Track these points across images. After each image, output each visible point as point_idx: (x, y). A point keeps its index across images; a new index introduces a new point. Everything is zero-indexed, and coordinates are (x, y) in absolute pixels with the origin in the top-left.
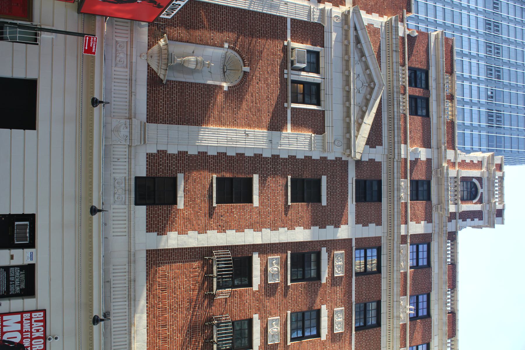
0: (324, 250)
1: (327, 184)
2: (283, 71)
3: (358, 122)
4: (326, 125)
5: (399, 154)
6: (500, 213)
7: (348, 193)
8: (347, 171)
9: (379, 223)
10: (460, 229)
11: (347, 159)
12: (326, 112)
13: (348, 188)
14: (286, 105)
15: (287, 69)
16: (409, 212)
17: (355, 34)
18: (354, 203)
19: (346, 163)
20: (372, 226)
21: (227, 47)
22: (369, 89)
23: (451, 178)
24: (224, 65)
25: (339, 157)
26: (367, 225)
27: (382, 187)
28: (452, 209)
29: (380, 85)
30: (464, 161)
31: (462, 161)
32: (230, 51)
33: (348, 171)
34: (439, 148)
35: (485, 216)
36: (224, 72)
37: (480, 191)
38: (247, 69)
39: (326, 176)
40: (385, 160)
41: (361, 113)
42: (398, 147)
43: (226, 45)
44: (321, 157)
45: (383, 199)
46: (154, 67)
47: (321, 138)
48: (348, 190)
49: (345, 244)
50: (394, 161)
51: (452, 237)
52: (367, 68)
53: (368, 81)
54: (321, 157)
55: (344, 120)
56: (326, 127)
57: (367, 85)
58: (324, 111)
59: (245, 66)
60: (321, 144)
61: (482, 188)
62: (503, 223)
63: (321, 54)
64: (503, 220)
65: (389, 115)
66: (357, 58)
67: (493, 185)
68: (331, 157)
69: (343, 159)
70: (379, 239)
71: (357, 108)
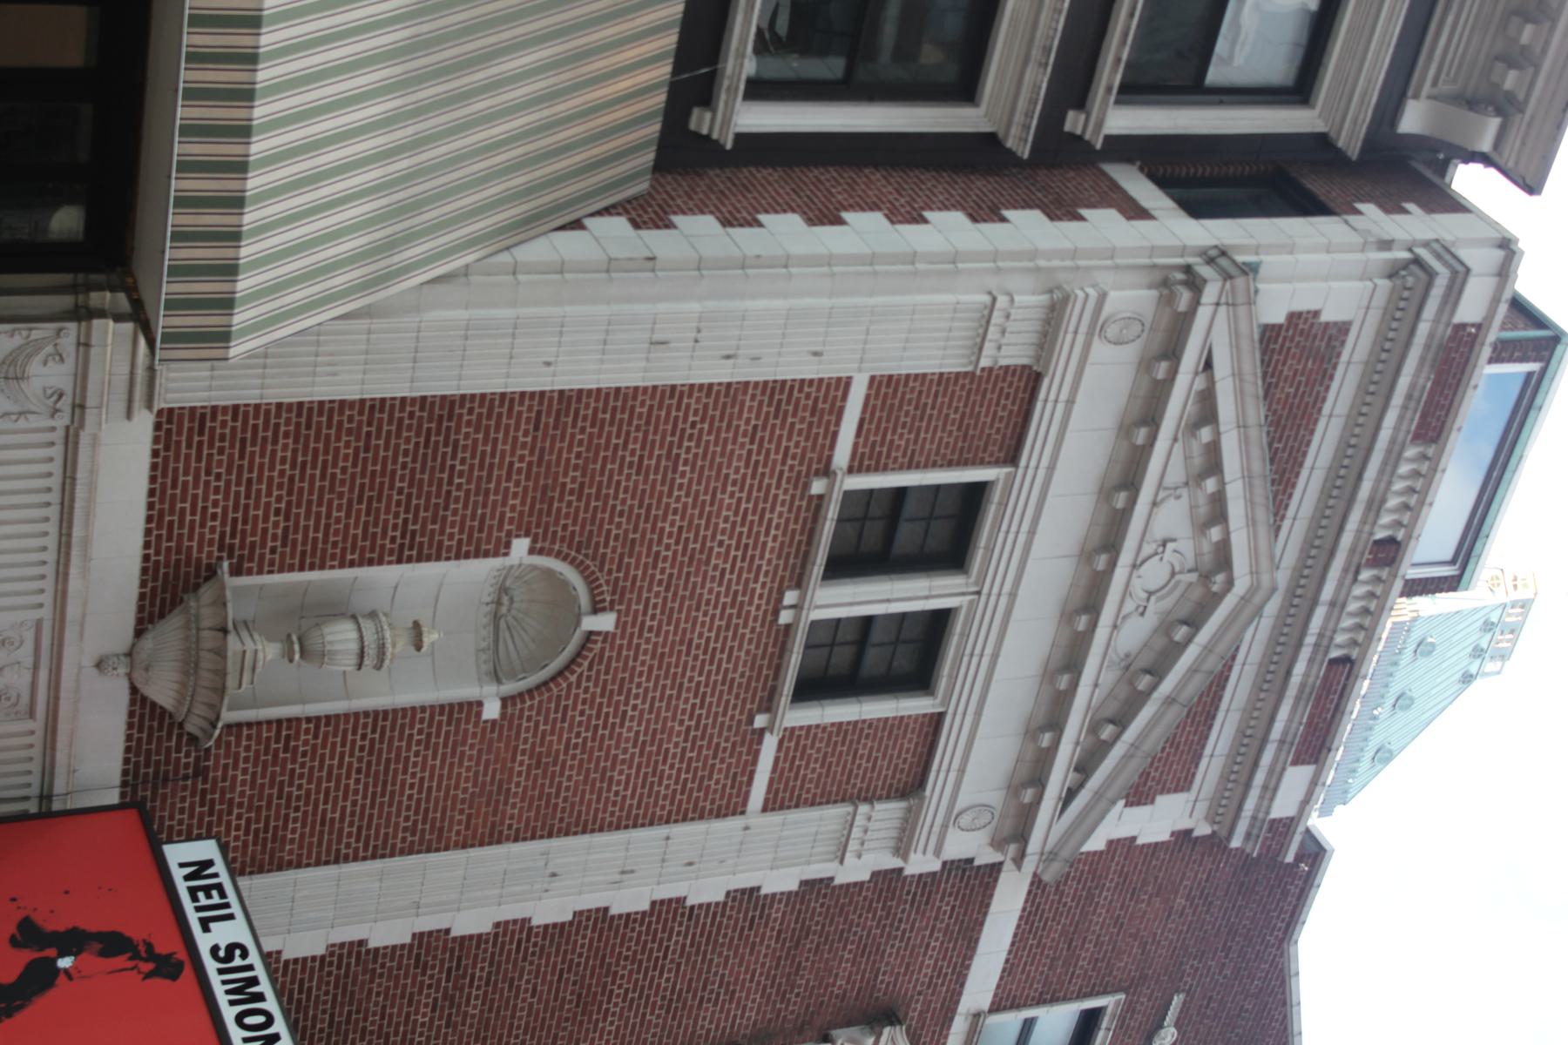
14: (760, 721)
29: (1253, 589)
36: (496, 617)
38: (605, 622)
41: (1123, 692)
43: (520, 546)
46: (163, 692)
47: (900, 814)
53: (1207, 558)
59: (596, 610)
71: (1109, 678)
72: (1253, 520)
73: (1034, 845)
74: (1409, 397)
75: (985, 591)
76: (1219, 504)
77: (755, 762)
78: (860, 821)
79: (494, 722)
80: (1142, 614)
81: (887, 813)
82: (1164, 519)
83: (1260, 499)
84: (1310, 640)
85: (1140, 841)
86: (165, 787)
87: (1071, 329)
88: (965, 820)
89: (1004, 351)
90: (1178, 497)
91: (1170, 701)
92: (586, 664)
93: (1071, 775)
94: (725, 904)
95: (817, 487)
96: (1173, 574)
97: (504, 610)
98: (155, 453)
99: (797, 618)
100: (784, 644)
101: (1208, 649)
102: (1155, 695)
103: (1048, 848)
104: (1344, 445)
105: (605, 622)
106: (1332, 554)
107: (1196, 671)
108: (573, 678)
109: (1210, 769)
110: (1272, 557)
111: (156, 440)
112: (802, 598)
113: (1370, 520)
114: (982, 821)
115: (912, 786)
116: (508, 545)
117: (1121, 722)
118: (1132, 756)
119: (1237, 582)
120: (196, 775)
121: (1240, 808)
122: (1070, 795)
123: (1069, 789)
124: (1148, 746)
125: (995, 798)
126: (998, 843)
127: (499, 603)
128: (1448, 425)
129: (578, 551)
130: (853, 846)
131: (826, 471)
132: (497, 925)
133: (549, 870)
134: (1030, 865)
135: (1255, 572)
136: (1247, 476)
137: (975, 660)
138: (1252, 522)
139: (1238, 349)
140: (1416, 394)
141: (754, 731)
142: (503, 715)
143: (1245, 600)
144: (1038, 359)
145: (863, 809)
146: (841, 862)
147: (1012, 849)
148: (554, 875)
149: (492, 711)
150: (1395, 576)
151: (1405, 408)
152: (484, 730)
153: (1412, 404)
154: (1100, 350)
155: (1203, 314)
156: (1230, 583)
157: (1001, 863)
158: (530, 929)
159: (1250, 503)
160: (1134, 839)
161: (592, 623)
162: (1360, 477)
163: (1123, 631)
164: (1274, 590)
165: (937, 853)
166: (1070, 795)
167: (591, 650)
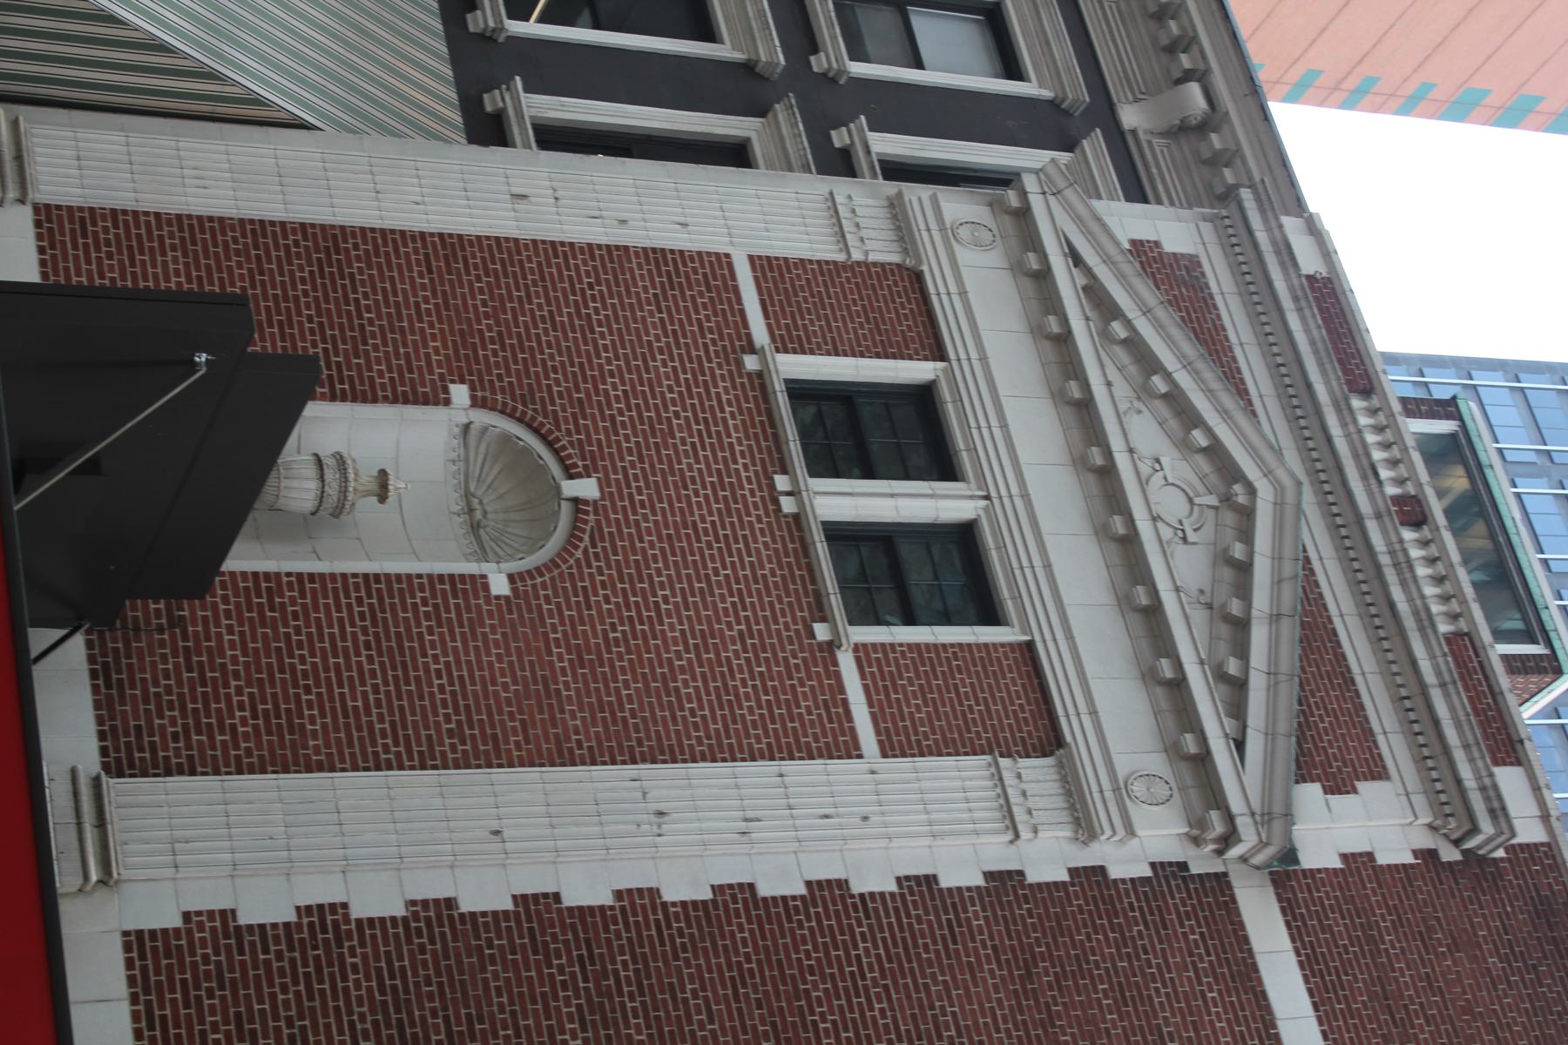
2: (772, 486)
3: (1221, 676)
14: (821, 632)
15: (784, 471)
17: (1081, 281)
21: (467, 402)
22: (1229, 518)
24: (468, 495)
29: (1279, 488)
32: (482, 417)
36: (475, 528)
38: (587, 488)
43: (460, 393)
44: (1073, 872)
52: (1189, 417)
57: (1212, 500)
58: (1029, 646)
59: (571, 477)
60: (1060, 802)
63: (945, 393)
66: (1122, 389)
71: (1199, 616)
72: (1226, 412)
73: (1236, 804)
74: (1296, 299)
75: (993, 494)
76: (1175, 400)
77: (842, 690)
78: (1008, 777)
79: (507, 598)
80: (1184, 539)
82: (1138, 435)
83: (1216, 385)
84: (1385, 560)
86: (138, 640)
87: (922, 226)
88: (1138, 788)
89: (869, 245)
90: (1140, 412)
91: (1275, 618)
92: (586, 538)
93: (1226, 721)
94: (902, 896)
95: (751, 363)
96: (1191, 501)
97: (478, 515)
98: (41, 250)
99: (801, 504)
100: (802, 539)
101: (1277, 558)
102: (1254, 613)
104: (1275, 368)
105: (587, 488)
106: (1340, 469)
107: (1280, 581)
108: (579, 554)
109: (1393, 745)
110: (1271, 447)
111: (39, 237)
112: (794, 481)
113: (1348, 420)
116: (446, 391)
118: (1276, 683)
119: (1256, 484)
120: (172, 625)
121: (1459, 781)
124: (1284, 667)
125: (1157, 763)
127: (471, 511)
128: (1371, 371)
129: (525, 405)
131: (751, 349)
132: (618, 894)
133: (653, 807)
135: (1268, 474)
136: (1188, 365)
137: (1028, 572)
138: (1225, 414)
139: (1091, 233)
140: (1300, 293)
141: (820, 644)
142: (514, 590)
143: (1279, 504)
144: (905, 251)
148: (661, 814)
149: (499, 585)
150: (1437, 529)
151: (1300, 310)
152: (499, 606)
153: (1303, 303)
154: (964, 255)
155: (1036, 202)
156: (1252, 491)
158: (664, 905)
159: (1209, 393)
161: (571, 488)
162: (1309, 386)
163: (1181, 572)
164: (1299, 484)
167: (586, 522)
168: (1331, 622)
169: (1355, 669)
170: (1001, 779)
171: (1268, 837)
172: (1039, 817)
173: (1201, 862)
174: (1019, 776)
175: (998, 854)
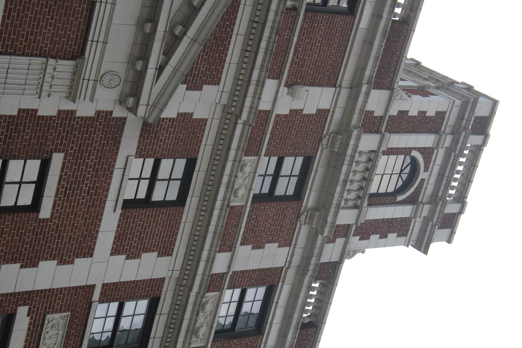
0: (22, 312)
1: (62, 170)
4: (90, 38)
5: (258, 96)
6: (450, 223)
7: (108, 190)
8: (117, 142)
9: (166, 250)
10: (350, 256)
11: (123, 115)
12: (98, 4)
13: (111, 178)
16: (243, 226)
18: (119, 211)
19: (123, 121)
20: (149, 258)
23: (360, 152)
25: (105, 109)
26: (137, 256)
27: (195, 173)
28: (346, 217)
30: (403, 113)
31: (400, 112)
33: (119, 143)
34: (355, 87)
35: (416, 227)
37: (423, 175)
39: (62, 155)
40: (218, 115)
42: (255, 93)
45: (189, 199)
47: (71, 69)
48: (109, 184)
49: (77, 302)
50: (236, 123)
51: (329, 274)
54: (60, 112)
55: (140, 24)
56: (89, 43)
60: (67, 83)
61: (426, 169)
62: (449, 241)
64: (452, 233)
65: (253, 14)
67: (454, 166)
68: (85, 109)
69: (114, 115)
70: (159, 283)
73: (143, 100)
78: (49, 70)
81: (66, 66)
85: (194, 117)
88: (106, 80)
93: (162, 56)
103: (151, 104)
114: (114, 83)
115: (78, 54)
117: (186, 23)
122: (160, 69)
123: (160, 66)
125: (121, 69)
126: (121, 102)
130: (46, 87)
134: (141, 111)
145: (51, 61)
146: (39, 97)
147: (131, 100)
157: (125, 119)
160: (192, 114)
165: (92, 100)
166: (160, 69)
168: (239, 7)
169: (235, 31)
170: (42, 86)
171: (148, 117)
172: (54, 88)
173: (118, 112)
174: (55, 69)
175: (29, 103)
